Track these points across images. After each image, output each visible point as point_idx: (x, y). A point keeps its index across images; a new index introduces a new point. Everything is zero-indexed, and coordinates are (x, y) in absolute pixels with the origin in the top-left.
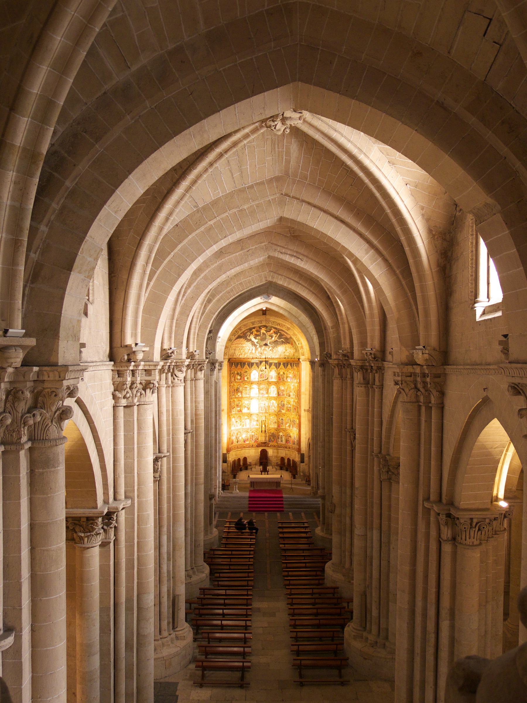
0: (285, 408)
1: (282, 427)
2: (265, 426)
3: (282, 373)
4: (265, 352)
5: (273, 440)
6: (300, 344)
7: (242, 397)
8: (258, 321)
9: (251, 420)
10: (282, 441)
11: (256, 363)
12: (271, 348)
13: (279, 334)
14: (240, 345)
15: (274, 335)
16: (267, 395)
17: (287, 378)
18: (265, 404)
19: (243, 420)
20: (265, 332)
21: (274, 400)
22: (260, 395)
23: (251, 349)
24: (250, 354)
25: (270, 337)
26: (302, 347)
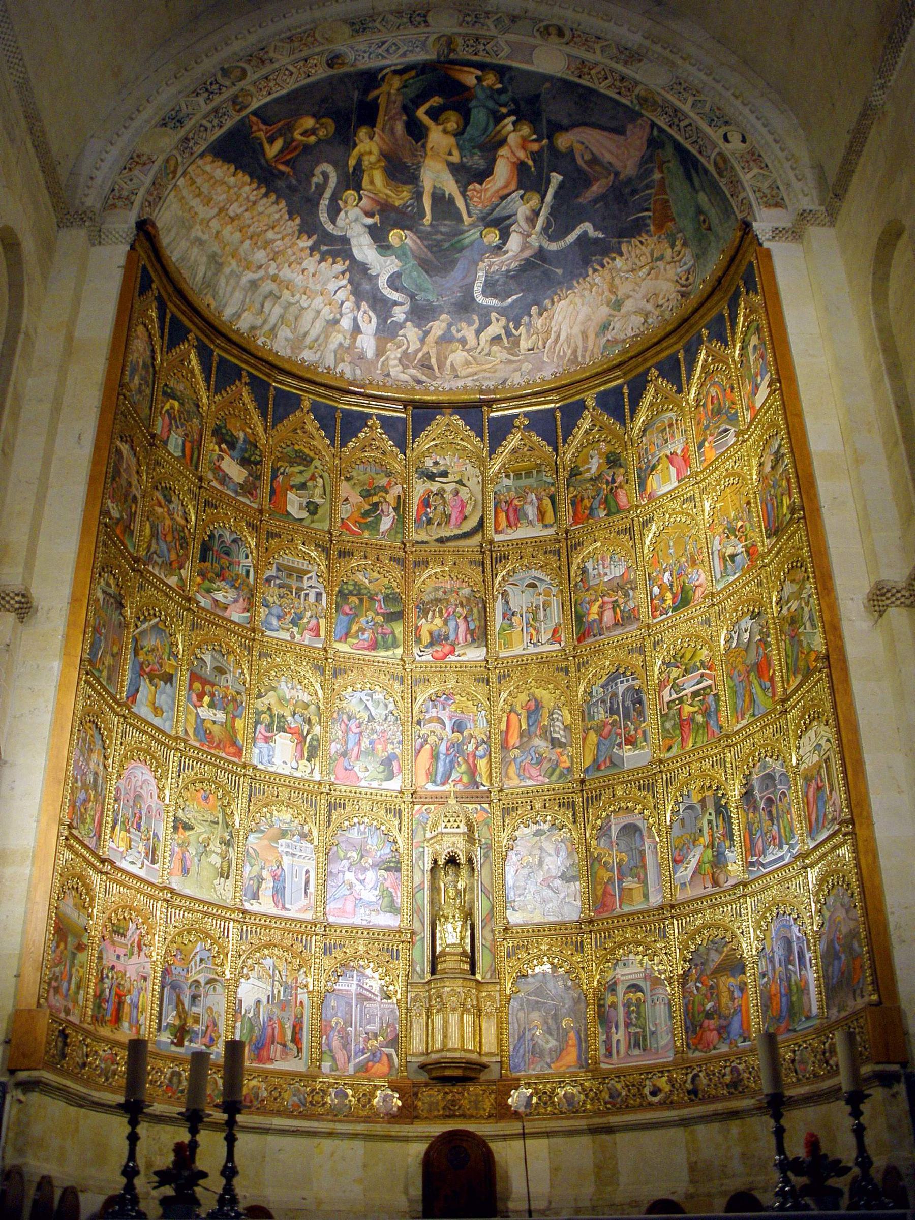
0: (651, 722)
1: (639, 905)
2: (468, 915)
3: (594, 465)
4: (458, 356)
5: (553, 1043)
6: (735, 138)
7: (253, 630)
8: (399, 13)
9: (328, 854)
10: (638, 1042)
11: (379, 417)
12: (495, 329)
13: (556, 178)
14: (260, 256)
15: (522, 210)
16: (476, 654)
17: (642, 484)
18: (458, 727)
19: (252, 837)
20: (451, 187)
21: (542, 682)
22: (416, 651)
23: (346, 323)
24: (339, 360)
25: (492, 237)
26: (755, 157)
